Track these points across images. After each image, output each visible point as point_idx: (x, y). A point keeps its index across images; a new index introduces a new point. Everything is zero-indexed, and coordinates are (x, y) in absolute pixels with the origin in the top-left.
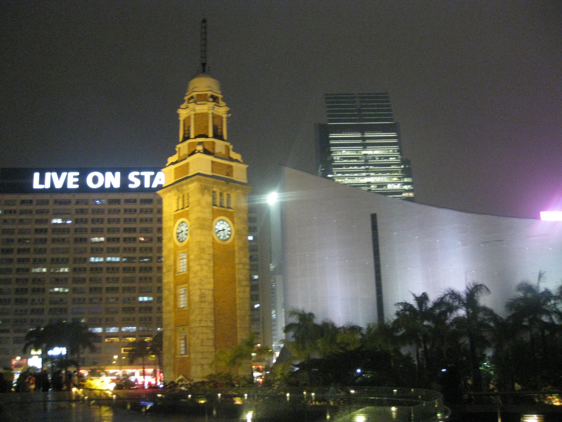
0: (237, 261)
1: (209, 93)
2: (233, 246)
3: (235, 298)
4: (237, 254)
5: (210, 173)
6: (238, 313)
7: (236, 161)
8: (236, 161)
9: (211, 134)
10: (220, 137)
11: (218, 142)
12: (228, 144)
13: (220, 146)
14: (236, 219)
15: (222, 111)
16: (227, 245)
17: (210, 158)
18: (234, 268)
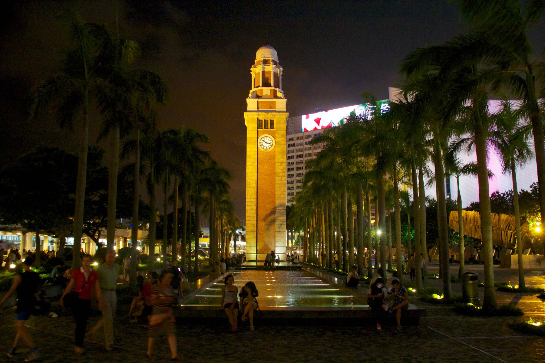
0: (277, 161)
1: (262, 59)
2: (275, 152)
3: (274, 184)
4: (276, 157)
5: (256, 110)
6: (276, 193)
7: (280, 98)
8: (280, 98)
9: (261, 85)
10: (269, 85)
11: (265, 89)
12: (273, 88)
13: (267, 91)
14: (276, 135)
15: (270, 68)
16: (270, 152)
17: (257, 100)
18: (274, 166)
